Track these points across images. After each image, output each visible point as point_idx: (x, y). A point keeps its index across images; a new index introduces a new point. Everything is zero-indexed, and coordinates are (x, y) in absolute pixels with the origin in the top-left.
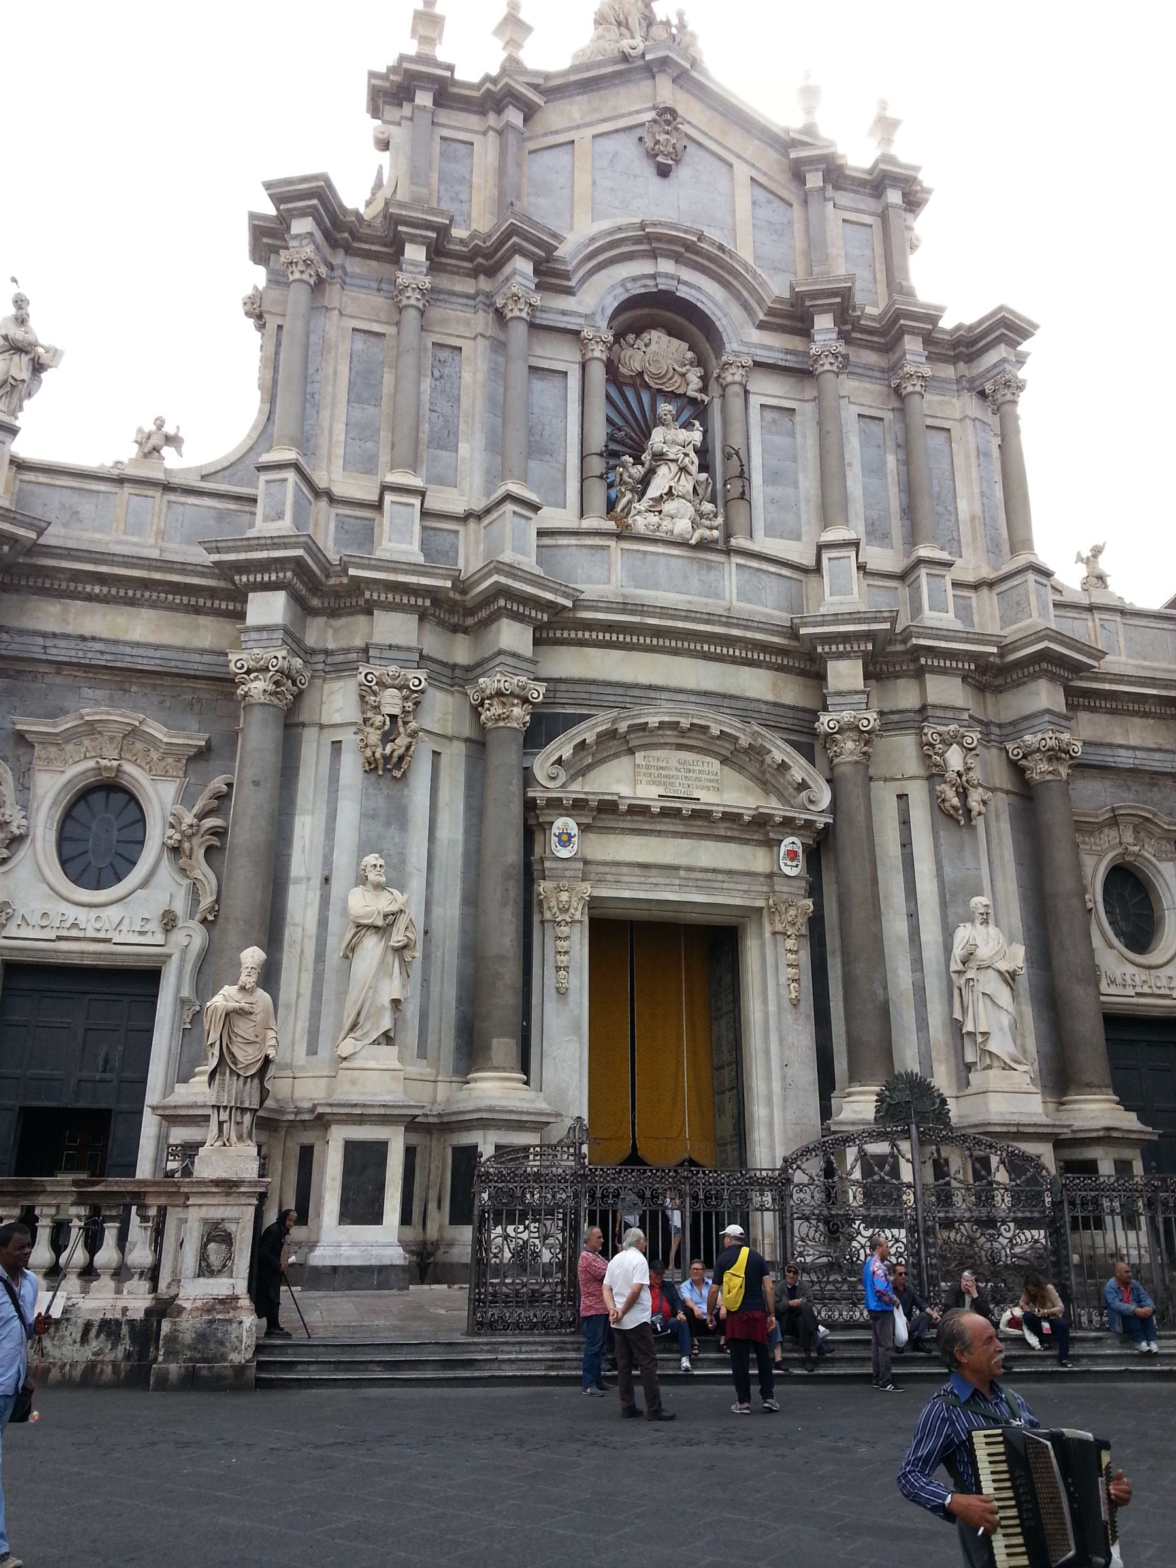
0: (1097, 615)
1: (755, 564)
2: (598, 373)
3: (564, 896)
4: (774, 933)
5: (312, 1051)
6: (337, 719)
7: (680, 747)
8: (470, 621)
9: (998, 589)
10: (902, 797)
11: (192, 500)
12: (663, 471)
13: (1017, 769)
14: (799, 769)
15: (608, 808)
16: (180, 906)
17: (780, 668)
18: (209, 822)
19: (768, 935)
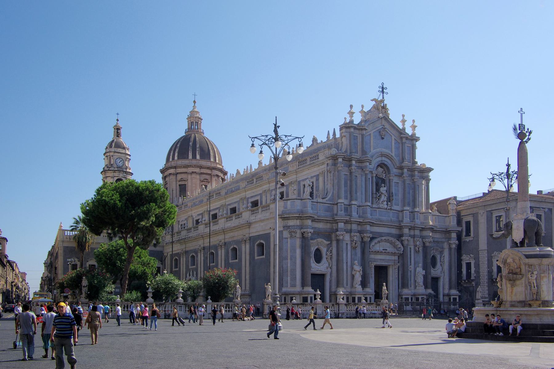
0: (435, 216)
1: (394, 211)
2: (374, 179)
3: (372, 264)
4: (395, 268)
5: (347, 285)
6: (347, 239)
7: (385, 242)
8: (361, 224)
9: (423, 214)
10: (410, 248)
11: (325, 205)
12: (383, 196)
13: (424, 243)
14: (400, 245)
15: (378, 252)
16: (328, 266)
17: (397, 228)
18: (331, 254)
19: (394, 269)
